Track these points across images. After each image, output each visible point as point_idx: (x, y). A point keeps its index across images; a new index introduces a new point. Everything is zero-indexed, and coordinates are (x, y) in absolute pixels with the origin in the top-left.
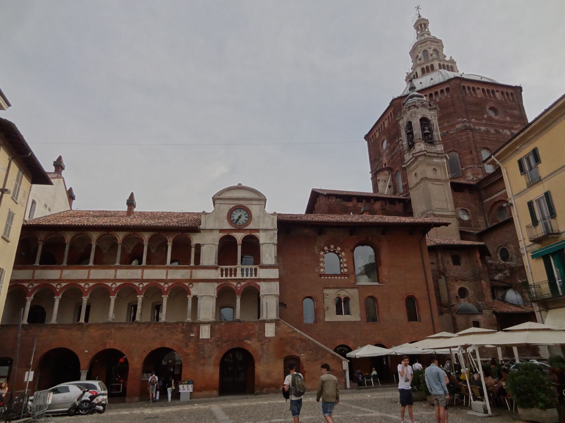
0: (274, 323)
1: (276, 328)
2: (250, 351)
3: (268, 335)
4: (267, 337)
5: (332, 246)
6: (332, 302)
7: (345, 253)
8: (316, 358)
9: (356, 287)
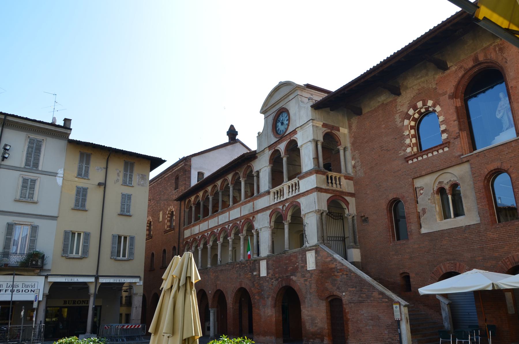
0: (314, 251)
1: (316, 258)
2: (295, 289)
3: (310, 267)
4: (309, 271)
5: (420, 104)
6: (429, 199)
7: (440, 105)
9: (465, 160)
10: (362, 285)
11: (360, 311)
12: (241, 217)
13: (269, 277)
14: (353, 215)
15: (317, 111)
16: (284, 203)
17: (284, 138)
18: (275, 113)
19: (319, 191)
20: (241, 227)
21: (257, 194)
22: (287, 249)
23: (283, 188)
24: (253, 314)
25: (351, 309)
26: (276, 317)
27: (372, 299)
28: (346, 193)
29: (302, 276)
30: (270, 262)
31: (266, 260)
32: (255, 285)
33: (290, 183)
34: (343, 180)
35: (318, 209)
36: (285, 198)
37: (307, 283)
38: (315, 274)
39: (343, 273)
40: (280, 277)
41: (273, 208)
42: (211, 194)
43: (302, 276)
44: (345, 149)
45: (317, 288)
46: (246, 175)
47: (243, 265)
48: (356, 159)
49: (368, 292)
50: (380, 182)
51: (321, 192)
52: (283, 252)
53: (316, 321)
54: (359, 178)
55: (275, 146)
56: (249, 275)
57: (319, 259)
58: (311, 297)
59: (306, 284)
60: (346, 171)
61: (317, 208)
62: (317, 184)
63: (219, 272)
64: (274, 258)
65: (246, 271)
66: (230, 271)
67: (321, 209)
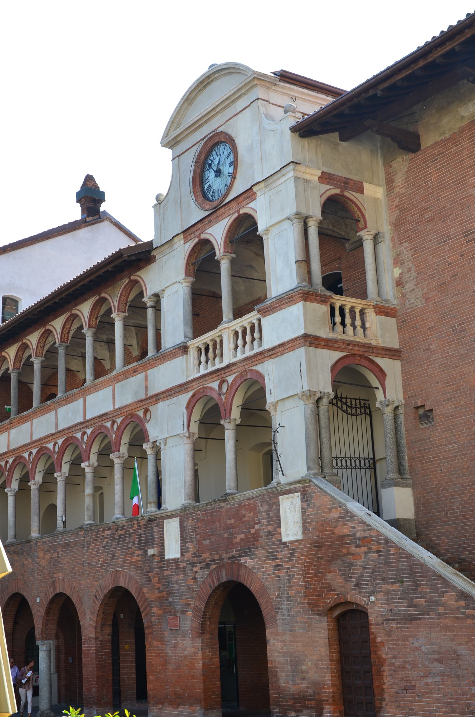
0: (299, 494)
1: (303, 511)
2: (252, 589)
3: (288, 535)
4: (285, 543)
8: (412, 610)
10: (416, 577)
11: (410, 639)
12: (115, 411)
13: (185, 559)
14: (396, 404)
15: (306, 141)
16: (224, 375)
17: (223, 210)
18: (200, 147)
19: (311, 344)
20: (114, 436)
21: (155, 351)
22: (232, 491)
23: (221, 336)
24: (146, 652)
25: (390, 636)
26: (203, 658)
27: (441, 609)
28: (378, 348)
29: (268, 556)
30: (189, 523)
31: (179, 518)
32: (151, 581)
33: (238, 324)
34: (371, 315)
35: (310, 391)
36: (226, 362)
37: (282, 573)
38: (300, 552)
39: (371, 548)
40: (214, 560)
41: (196, 387)
42: (38, 353)
43: (268, 556)
44: (376, 239)
45: (306, 585)
46: (126, 304)
47: (122, 532)
48: (404, 263)
49: (431, 592)
50: (464, 320)
51: (316, 347)
52: (222, 497)
53: (304, 668)
54: (410, 312)
55: (199, 229)
56: (138, 556)
57: (311, 515)
58: (291, 608)
59: (279, 576)
60: (379, 295)
61: (306, 388)
62: (306, 328)
63: (61, 550)
64: (199, 512)
65: (130, 545)
66: (88, 547)
67: (317, 390)
